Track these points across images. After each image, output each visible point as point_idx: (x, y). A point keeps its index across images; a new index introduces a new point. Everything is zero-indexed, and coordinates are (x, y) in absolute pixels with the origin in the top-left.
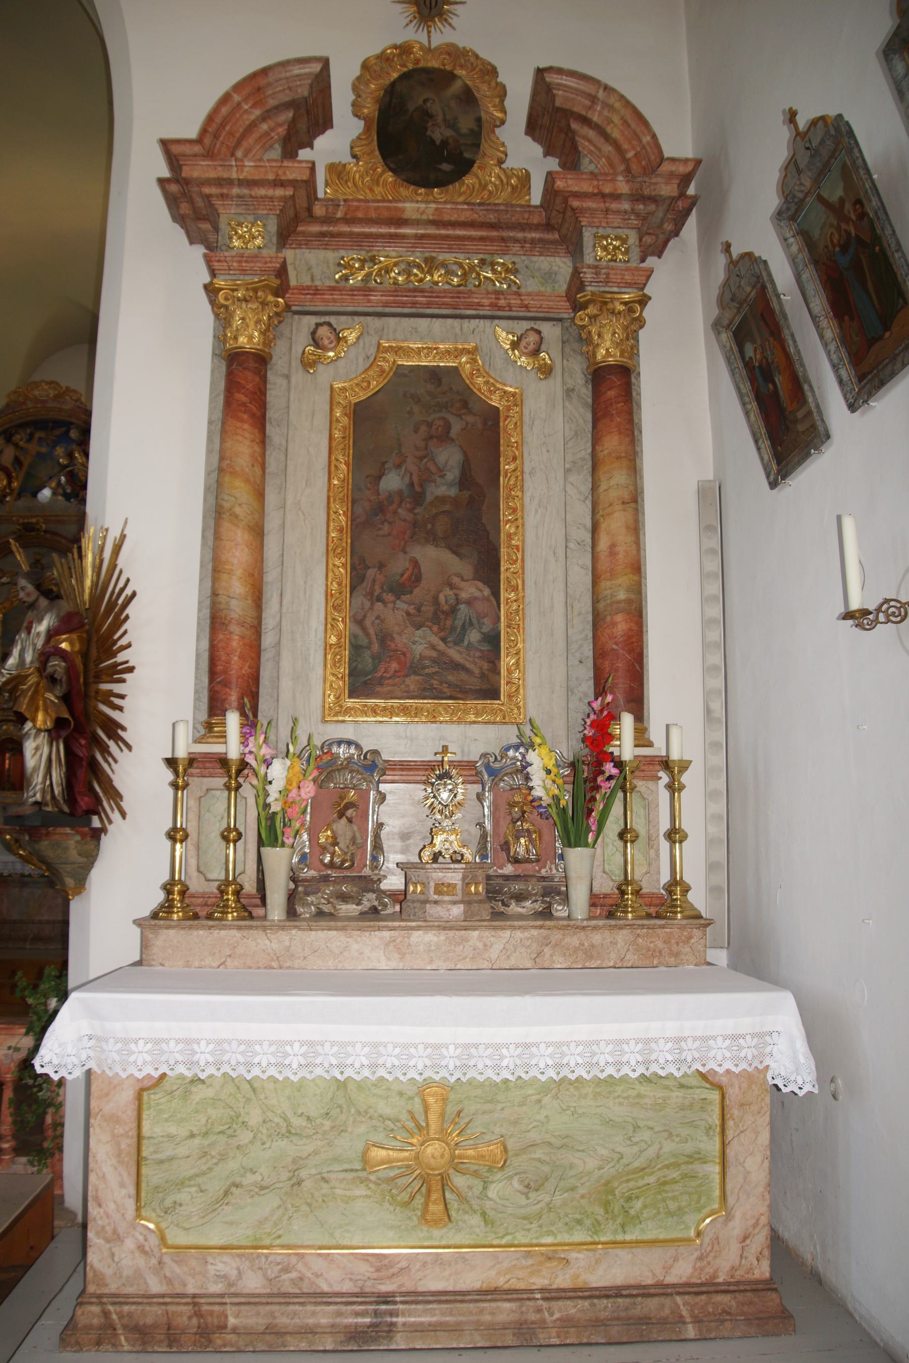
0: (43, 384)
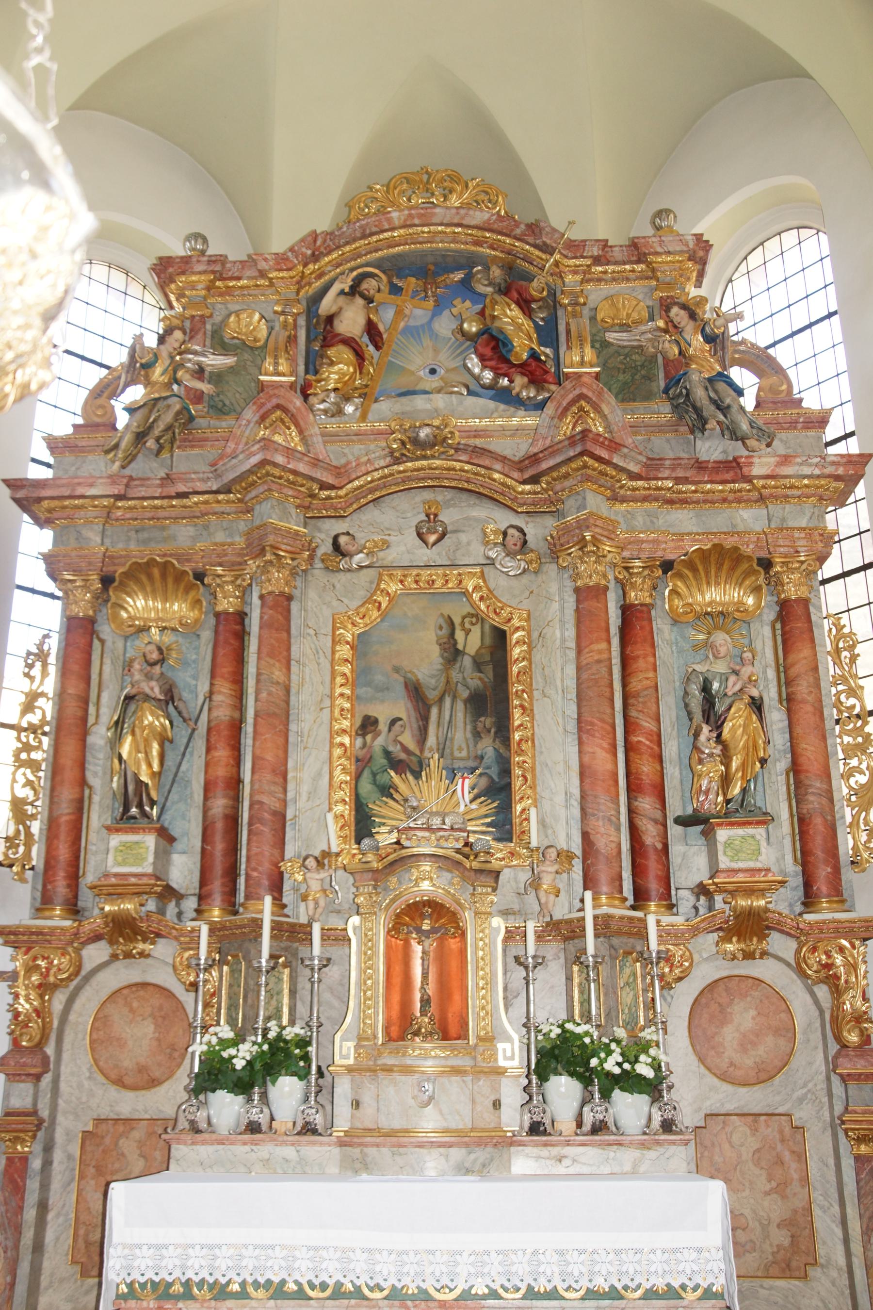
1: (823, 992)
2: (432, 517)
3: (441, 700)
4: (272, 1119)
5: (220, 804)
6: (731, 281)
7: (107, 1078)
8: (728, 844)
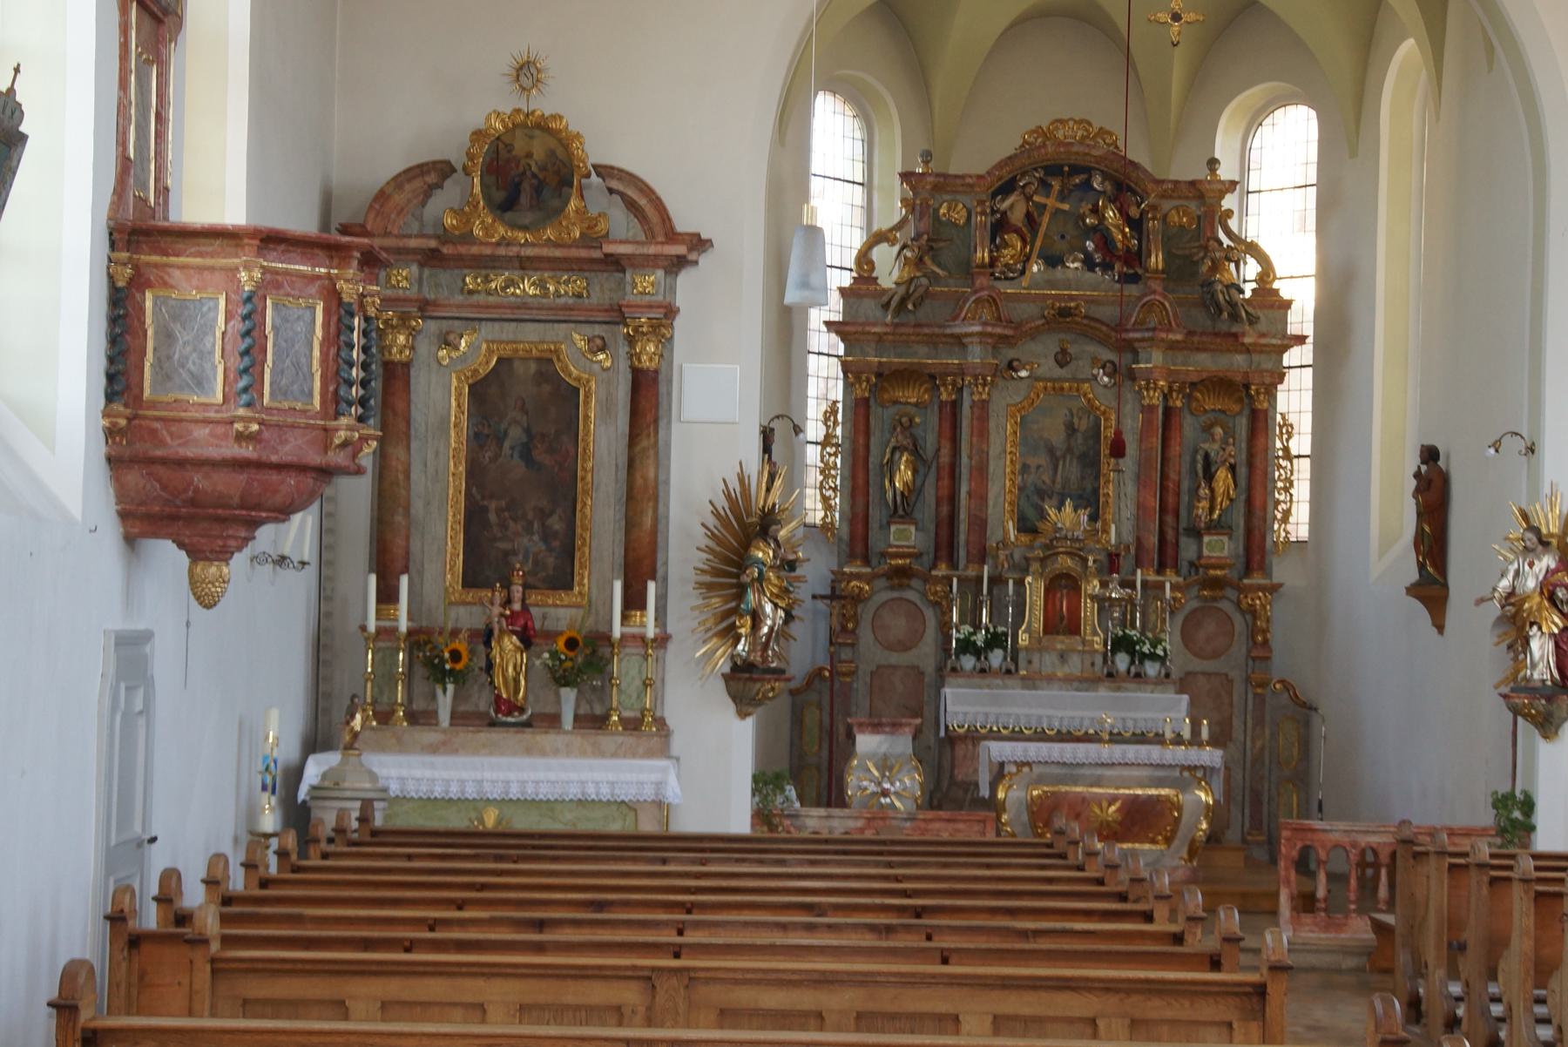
0: (1071, 123)
1: (1248, 617)
2: (1064, 351)
3: (1064, 457)
4: (990, 667)
5: (945, 510)
8: (1209, 543)
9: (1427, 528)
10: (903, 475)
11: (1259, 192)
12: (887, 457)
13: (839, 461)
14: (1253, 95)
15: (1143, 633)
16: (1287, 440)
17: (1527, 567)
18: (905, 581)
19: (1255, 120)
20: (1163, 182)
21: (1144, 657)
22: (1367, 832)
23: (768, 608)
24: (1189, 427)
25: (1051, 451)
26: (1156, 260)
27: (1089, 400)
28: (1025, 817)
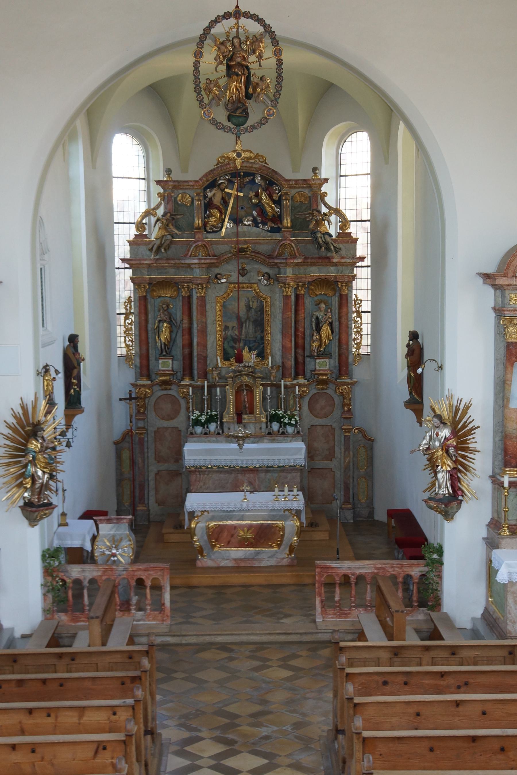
1: (341, 398)
2: (243, 269)
3: (246, 322)
4: (210, 431)
5: (187, 351)
6: (345, 141)
7: (160, 418)
8: (319, 363)
9: (412, 375)
10: (165, 335)
11: (346, 176)
12: (156, 325)
13: (133, 327)
14: (340, 127)
15: (285, 412)
16: (359, 308)
17: (435, 436)
18: (169, 387)
19: (342, 139)
20: (290, 180)
21: (285, 424)
22: (359, 568)
23: (40, 473)
24: (309, 303)
25: (238, 318)
26: (287, 221)
27: (257, 293)
28: (206, 538)
